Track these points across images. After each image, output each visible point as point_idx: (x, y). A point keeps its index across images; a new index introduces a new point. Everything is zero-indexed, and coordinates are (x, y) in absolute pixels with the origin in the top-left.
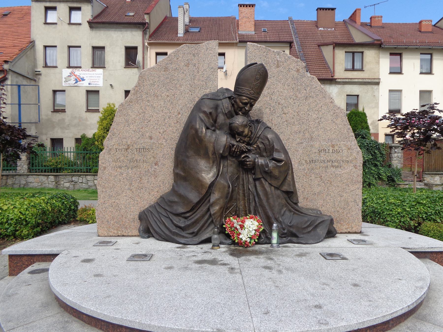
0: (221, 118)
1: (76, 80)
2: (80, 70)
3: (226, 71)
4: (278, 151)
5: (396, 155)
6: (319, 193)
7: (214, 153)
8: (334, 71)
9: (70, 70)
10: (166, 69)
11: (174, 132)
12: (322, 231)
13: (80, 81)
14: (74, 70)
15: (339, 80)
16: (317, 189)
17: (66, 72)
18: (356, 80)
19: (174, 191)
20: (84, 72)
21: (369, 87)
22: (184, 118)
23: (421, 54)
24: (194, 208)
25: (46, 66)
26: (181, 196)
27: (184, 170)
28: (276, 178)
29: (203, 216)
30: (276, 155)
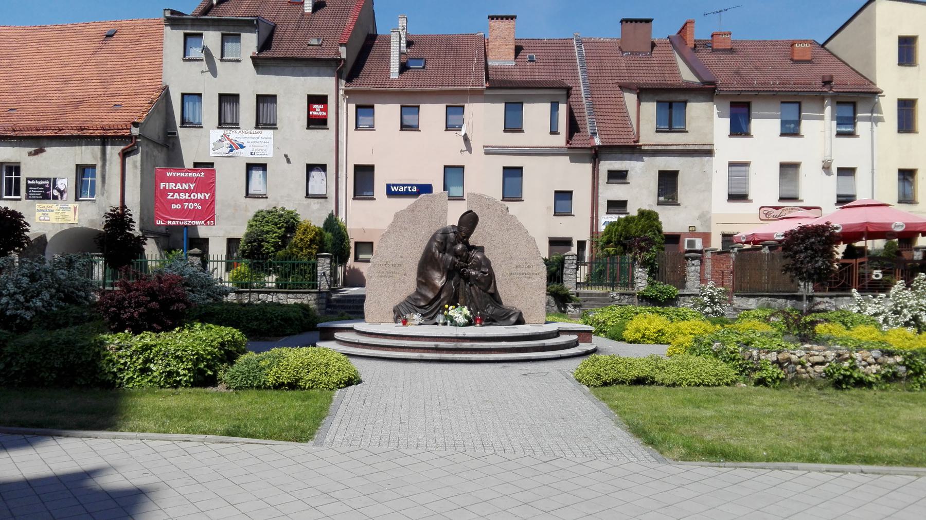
0: (448, 246)
1: (231, 146)
2: (238, 131)
3: (466, 134)
4: (484, 267)
5: (693, 268)
6: (516, 296)
7: (445, 267)
8: (638, 132)
9: (222, 131)
10: (413, 211)
11: (417, 254)
12: (513, 319)
13: (237, 148)
14: (228, 131)
15: (646, 148)
16: (515, 293)
17: (216, 134)
18: (674, 148)
19: (417, 292)
20: (244, 135)
21: (696, 160)
22: (424, 244)
23: (782, 102)
24: (431, 303)
25: (184, 123)
26: (422, 295)
27: (426, 279)
28: (482, 284)
29: (436, 308)
30: (483, 270)
